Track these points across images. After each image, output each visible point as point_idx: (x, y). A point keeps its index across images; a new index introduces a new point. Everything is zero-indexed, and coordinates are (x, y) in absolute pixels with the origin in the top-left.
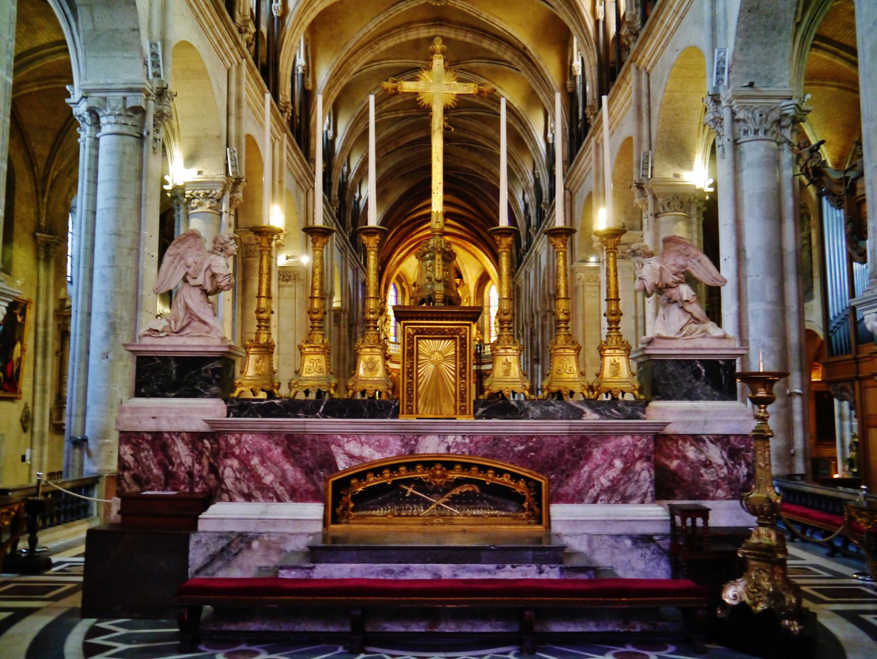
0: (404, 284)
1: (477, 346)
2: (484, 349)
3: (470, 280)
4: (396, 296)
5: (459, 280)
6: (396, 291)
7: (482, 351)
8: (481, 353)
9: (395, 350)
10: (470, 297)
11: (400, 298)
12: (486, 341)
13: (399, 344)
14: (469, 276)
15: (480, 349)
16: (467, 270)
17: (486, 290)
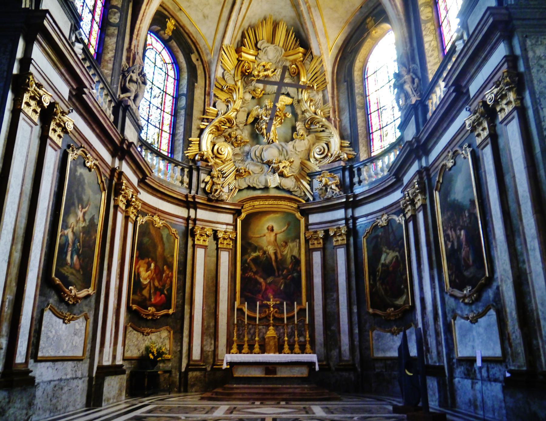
0: (194, 57)
1: (344, 169)
2: (359, 175)
3: (324, 47)
4: (178, 80)
5: (301, 49)
6: (178, 71)
7: (356, 180)
8: (352, 184)
9: (165, 174)
10: (324, 82)
11: (184, 82)
12: (363, 156)
13: (177, 164)
14: (322, 39)
15: (352, 176)
16: (319, 24)
17: (358, 64)
